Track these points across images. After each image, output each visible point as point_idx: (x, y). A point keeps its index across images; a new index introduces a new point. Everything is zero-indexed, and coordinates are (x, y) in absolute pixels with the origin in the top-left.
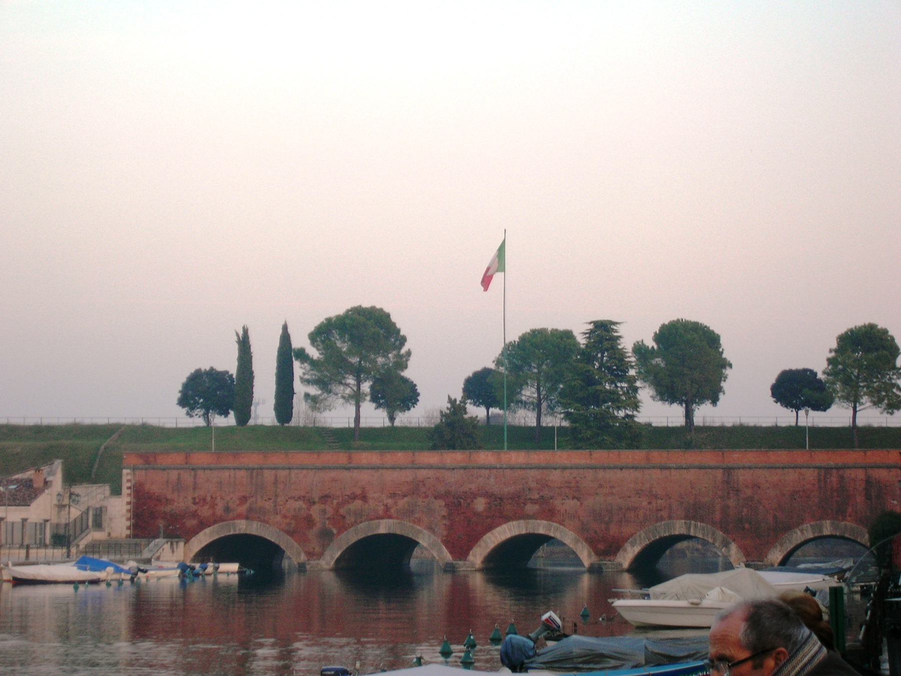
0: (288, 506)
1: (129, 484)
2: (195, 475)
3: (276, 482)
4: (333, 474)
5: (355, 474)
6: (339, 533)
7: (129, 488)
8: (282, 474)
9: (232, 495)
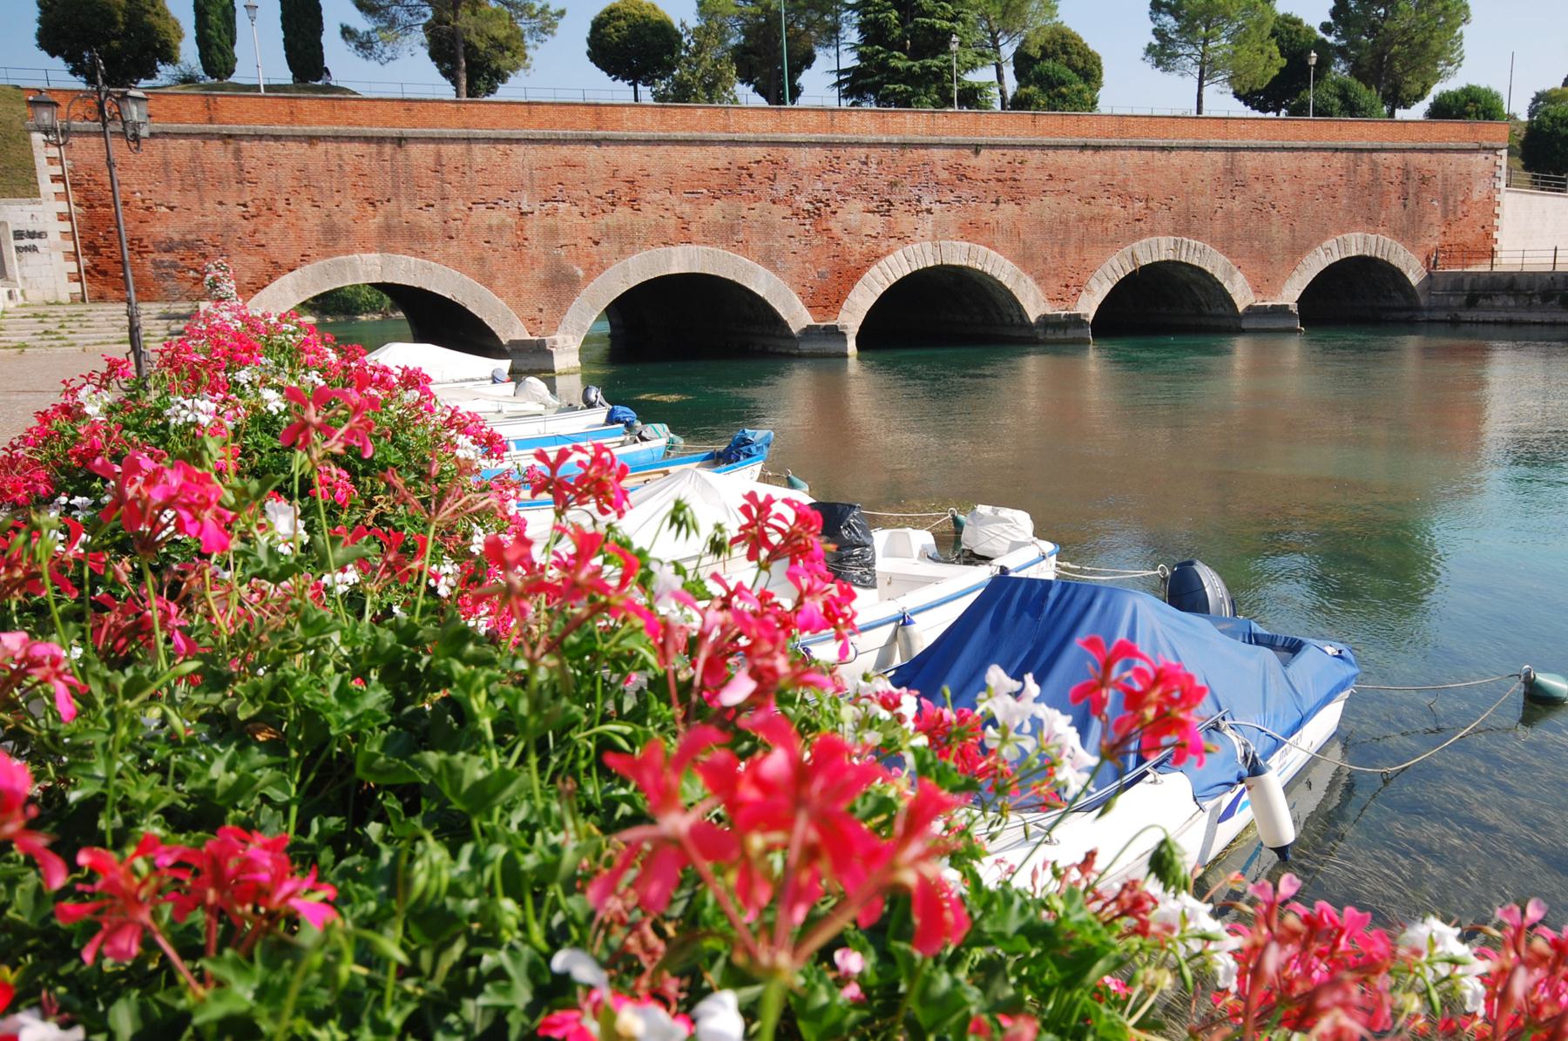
0: (473, 220)
1: (57, 170)
2: (238, 153)
3: (438, 167)
4: (565, 151)
5: (612, 152)
6: (589, 277)
7: (55, 179)
8: (450, 150)
9: (338, 197)
